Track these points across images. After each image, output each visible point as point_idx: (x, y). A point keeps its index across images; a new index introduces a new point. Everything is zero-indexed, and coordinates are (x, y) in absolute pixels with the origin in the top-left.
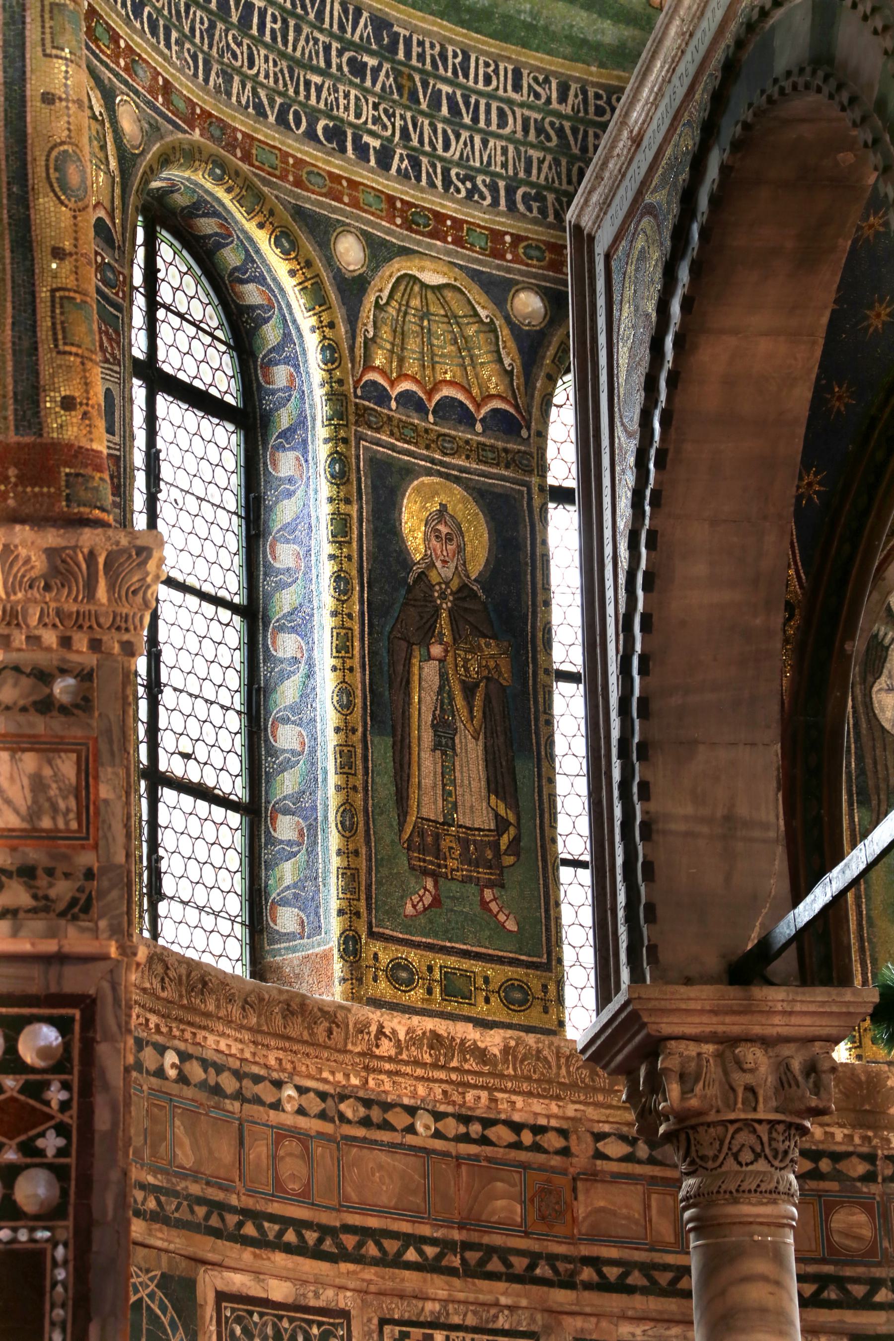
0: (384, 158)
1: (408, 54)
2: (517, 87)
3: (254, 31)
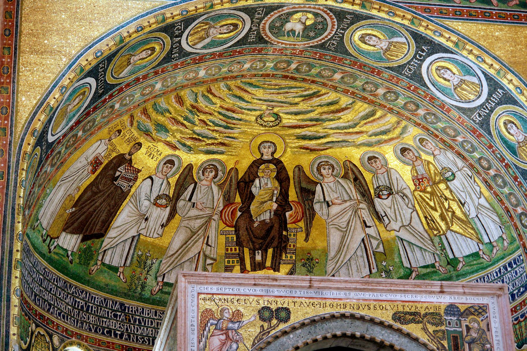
0: (121, 336)
1: (128, 311)
2: (156, 315)
3: (90, 311)
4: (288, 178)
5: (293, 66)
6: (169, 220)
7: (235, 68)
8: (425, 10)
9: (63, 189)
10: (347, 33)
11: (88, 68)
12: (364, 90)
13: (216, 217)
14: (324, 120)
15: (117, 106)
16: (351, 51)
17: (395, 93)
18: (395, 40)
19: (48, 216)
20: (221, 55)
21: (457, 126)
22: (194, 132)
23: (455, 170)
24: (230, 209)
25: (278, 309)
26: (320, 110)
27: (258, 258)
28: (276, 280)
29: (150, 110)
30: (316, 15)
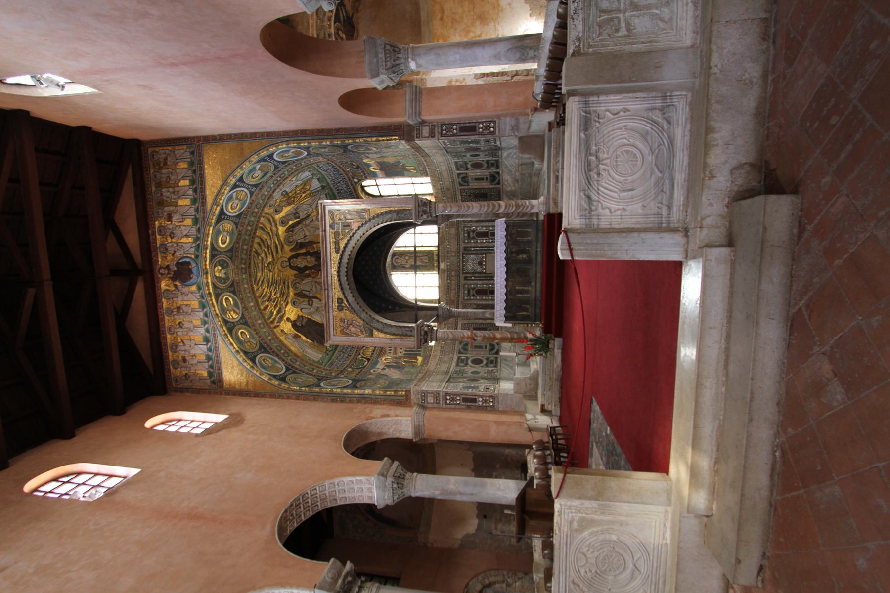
4: (295, 254)
5: (243, 266)
7: (247, 291)
8: (204, 220)
9: (306, 350)
11: (251, 364)
12: (250, 235)
13: (315, 279)
14: (268, 245)
15: (270, 338)
16: (231, 246)
17: (249, 222)
18: (222, 230)
19: (317, 355)
20: (242, 300)
21: (260, 195)
22: (280, 296)
23: (281, 192)
24: (311, 274)
25: (338, 303)
26: (263, 248)
28: (326, 304)
30: (215, 267)
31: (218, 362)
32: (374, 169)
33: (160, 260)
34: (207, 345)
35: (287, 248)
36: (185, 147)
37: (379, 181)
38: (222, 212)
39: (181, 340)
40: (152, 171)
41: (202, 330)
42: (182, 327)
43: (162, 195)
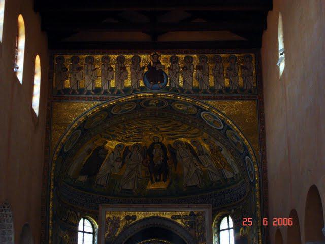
6: (122, 167)
8: (199, 97)
10: (172, 105)
15: (93, 133)
20: (128, 113)
25: (132, 216)
27: (158, 178)
29: (108, 132)
31: (78, 98)
32: (242, 231)
33: (165, 56)
34: (93, 90)
35: (172, 142)
36: (255, 85)
37: (232, 231)
38: (203, 110)
39: (97, 68)
40: (236, 55)
41: (105, 88)
42: (108, 69)
43: (218, 62)
